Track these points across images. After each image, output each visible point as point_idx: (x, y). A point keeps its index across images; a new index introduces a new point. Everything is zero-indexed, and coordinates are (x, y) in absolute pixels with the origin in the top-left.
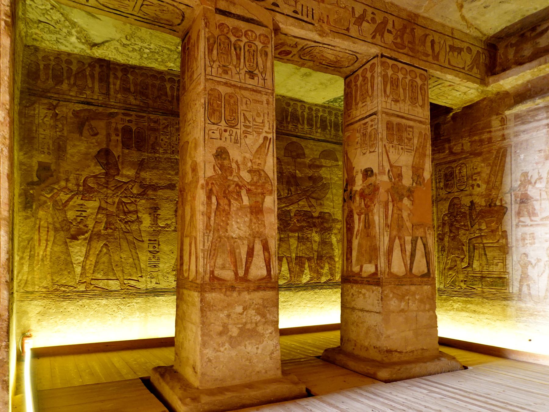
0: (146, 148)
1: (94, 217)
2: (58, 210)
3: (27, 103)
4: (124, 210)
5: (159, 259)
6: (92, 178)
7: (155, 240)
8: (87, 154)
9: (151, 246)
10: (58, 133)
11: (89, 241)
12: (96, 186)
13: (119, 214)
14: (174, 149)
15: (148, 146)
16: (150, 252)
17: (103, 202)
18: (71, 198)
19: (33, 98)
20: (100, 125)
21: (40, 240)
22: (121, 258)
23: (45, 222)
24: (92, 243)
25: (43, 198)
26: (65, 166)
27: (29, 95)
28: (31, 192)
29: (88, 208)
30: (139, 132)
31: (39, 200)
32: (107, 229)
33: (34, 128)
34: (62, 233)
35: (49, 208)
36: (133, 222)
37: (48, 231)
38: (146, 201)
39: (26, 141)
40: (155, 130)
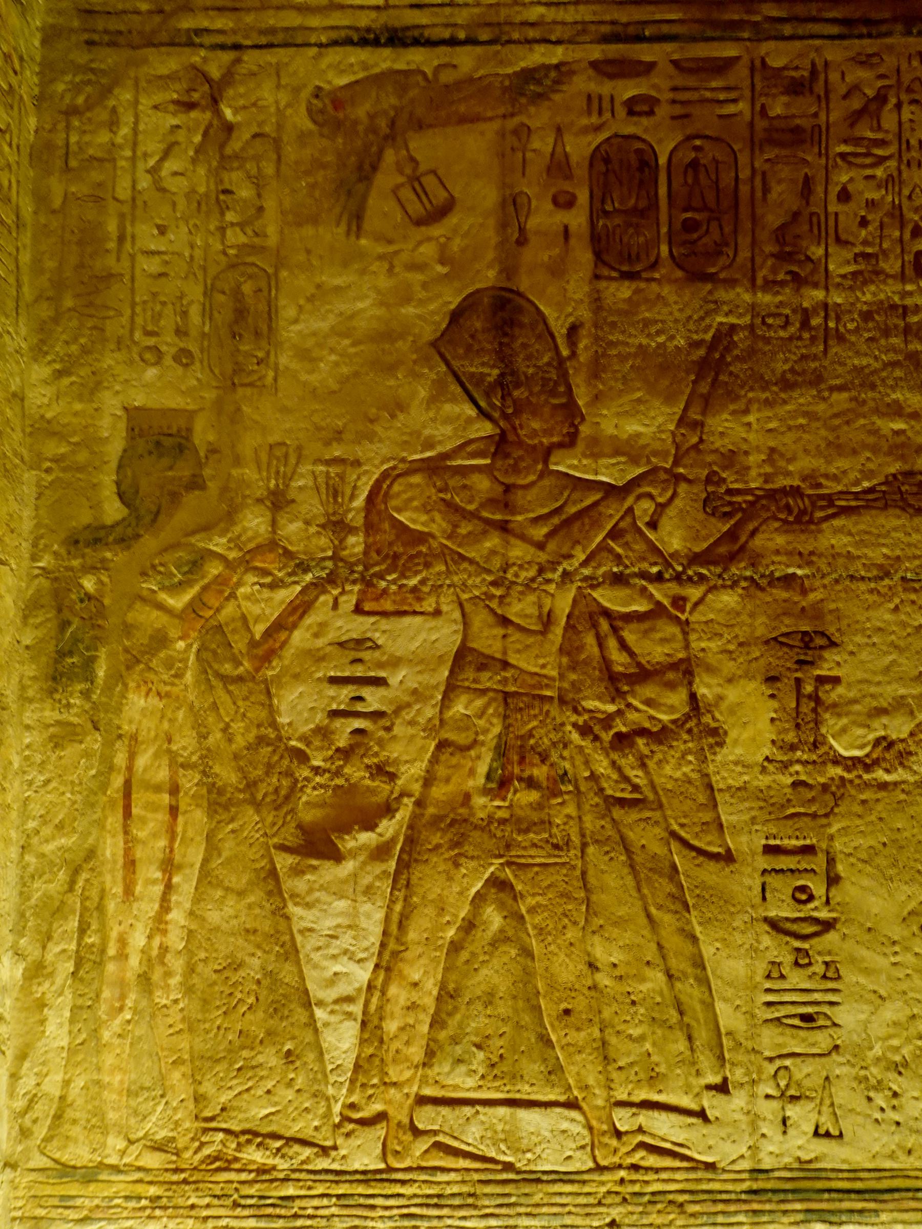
0: (744, 254)
1: (430, 712)
2: (225, 679)
3: (76, 89)
4: (606, 663)
5: (831, 972)
6: (416, 479)
7: (808, 850)
8: (386, 335)
9: (783, 887)
10: (235, 237)
11: (404, 865)
12: (434, 525)
13: (576, 687)
15: (754, 243)
16: (774, 925)
17: (480, 618)
18: (300, 608)
19: (109, 58)
20: (463, 155)
21: (130, 864)
22: (593, 966)
23: (156, 756)
24: (417, 873)
25: (148, 618)
26: (272, 419)
27: (90, 43)
28: (89, 584)
29: (395, 663)
30: (694, 165)
31: (128, 629)
32: (504, 784)
33: (112, 227)
34: (250, 815)
35: (179, 675)
36: (661, 736)
37: (174, 811)
38: (747, 595)
39: (69, 302)
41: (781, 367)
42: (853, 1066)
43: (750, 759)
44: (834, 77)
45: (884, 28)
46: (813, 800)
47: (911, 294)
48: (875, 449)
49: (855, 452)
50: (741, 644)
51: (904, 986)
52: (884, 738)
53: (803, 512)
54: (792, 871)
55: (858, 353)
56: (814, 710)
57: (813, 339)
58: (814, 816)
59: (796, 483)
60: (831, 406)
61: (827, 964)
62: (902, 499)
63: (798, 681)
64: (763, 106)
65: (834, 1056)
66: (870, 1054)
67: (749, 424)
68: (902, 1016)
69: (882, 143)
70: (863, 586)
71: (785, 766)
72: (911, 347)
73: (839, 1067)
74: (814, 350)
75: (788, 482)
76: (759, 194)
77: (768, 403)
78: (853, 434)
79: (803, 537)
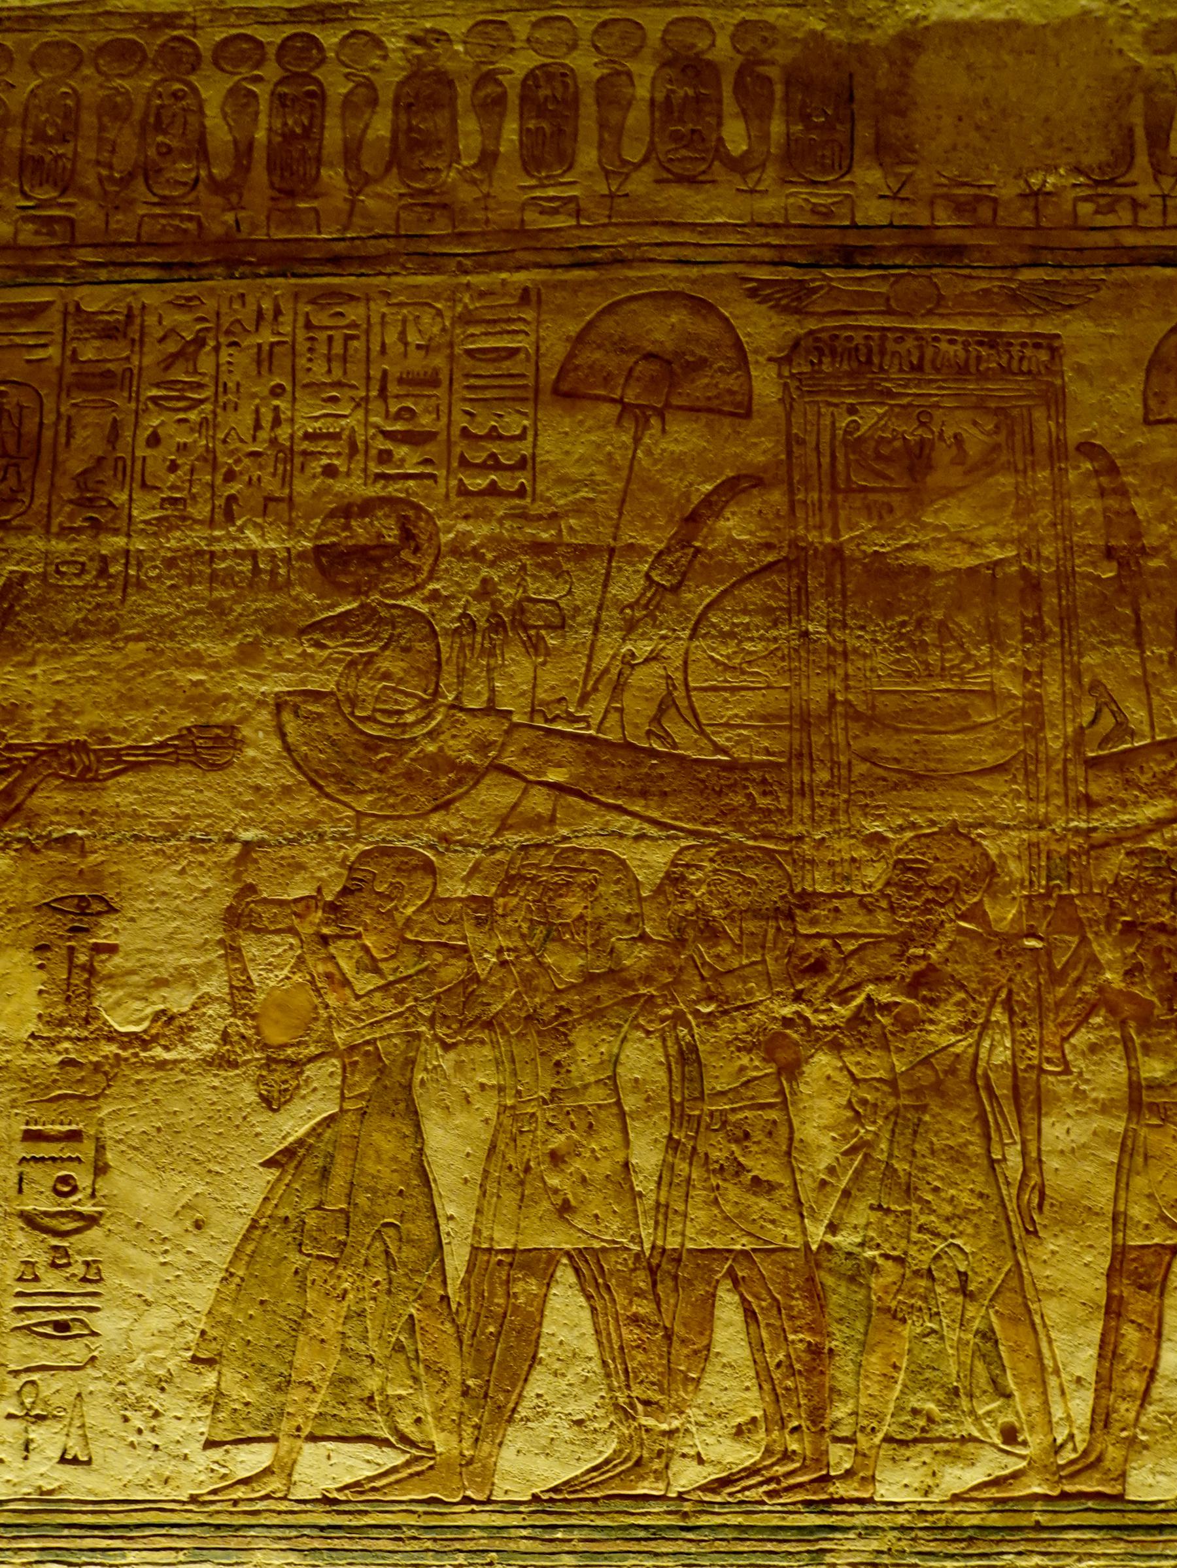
0: (41, 500)
5: (92, 1276)
9: (44, 1177)
14: (235, 488)
16: (31, 1221)
38: (20, 858)
40: (102, 381)
41: (73, 616)
42: (109, 1381)
43: (14, 1036)
44: (151, 320)
45: (205, 272)
46: (81, 1081)
47: (218, 539)
48: (169, 702)
49: (147, 704)
50: (10, 911)
51: (172, 1289)
52: (163, 1012)
53: (88, 769)
54: (53, 1159)
55: (159, 602)
56: (87, 982)
57: (110, 587)
58: (82, 1098)
59: (82, 738)
60: (126, 656)
61: (87, 1264)
62: (196, 754)
63: (71, 949)
64: (74, 351)
65: (89, 1370)
66: (131, 1367)
67: (34, 676)
68: (167, 1325)
69: (200, 386)
70: (147, 847)
71: (52, 1042)
72: (216, 594)
73: (94, 1383)
74: (111, 598)
75: (73, 737)
76: (63, 440)
77: (56, 654)
78: (150, 685)
79: (85, 795)
